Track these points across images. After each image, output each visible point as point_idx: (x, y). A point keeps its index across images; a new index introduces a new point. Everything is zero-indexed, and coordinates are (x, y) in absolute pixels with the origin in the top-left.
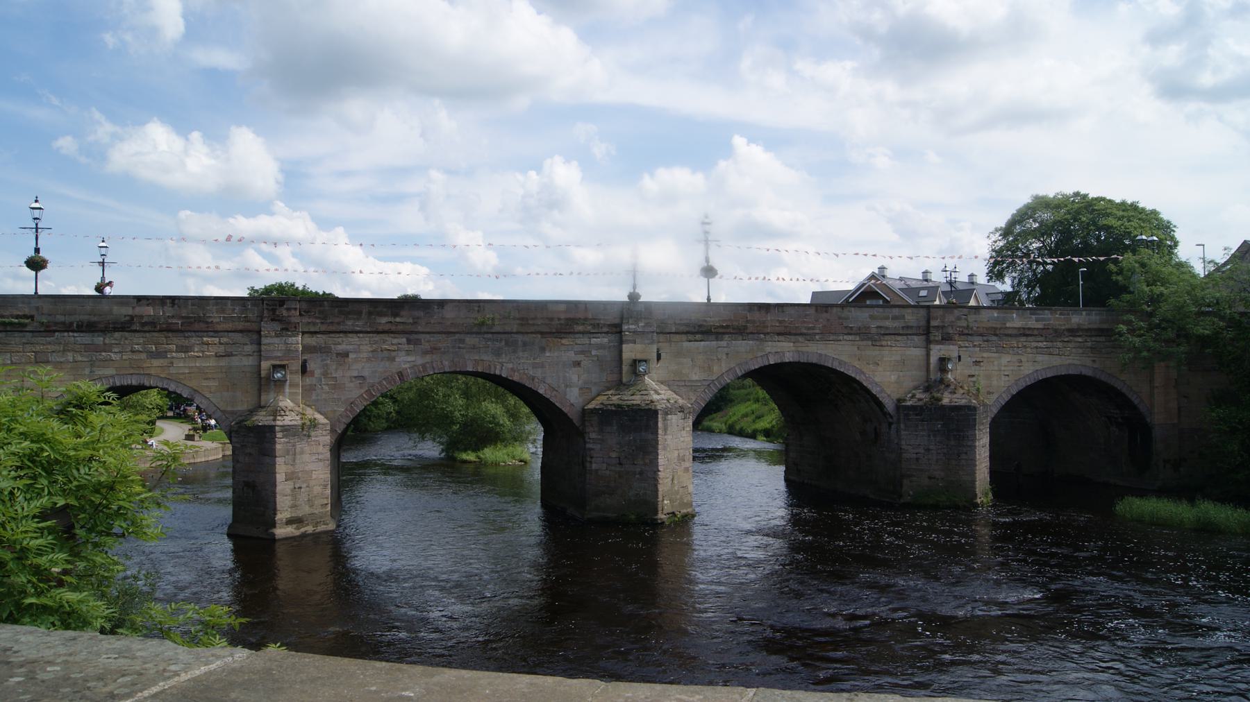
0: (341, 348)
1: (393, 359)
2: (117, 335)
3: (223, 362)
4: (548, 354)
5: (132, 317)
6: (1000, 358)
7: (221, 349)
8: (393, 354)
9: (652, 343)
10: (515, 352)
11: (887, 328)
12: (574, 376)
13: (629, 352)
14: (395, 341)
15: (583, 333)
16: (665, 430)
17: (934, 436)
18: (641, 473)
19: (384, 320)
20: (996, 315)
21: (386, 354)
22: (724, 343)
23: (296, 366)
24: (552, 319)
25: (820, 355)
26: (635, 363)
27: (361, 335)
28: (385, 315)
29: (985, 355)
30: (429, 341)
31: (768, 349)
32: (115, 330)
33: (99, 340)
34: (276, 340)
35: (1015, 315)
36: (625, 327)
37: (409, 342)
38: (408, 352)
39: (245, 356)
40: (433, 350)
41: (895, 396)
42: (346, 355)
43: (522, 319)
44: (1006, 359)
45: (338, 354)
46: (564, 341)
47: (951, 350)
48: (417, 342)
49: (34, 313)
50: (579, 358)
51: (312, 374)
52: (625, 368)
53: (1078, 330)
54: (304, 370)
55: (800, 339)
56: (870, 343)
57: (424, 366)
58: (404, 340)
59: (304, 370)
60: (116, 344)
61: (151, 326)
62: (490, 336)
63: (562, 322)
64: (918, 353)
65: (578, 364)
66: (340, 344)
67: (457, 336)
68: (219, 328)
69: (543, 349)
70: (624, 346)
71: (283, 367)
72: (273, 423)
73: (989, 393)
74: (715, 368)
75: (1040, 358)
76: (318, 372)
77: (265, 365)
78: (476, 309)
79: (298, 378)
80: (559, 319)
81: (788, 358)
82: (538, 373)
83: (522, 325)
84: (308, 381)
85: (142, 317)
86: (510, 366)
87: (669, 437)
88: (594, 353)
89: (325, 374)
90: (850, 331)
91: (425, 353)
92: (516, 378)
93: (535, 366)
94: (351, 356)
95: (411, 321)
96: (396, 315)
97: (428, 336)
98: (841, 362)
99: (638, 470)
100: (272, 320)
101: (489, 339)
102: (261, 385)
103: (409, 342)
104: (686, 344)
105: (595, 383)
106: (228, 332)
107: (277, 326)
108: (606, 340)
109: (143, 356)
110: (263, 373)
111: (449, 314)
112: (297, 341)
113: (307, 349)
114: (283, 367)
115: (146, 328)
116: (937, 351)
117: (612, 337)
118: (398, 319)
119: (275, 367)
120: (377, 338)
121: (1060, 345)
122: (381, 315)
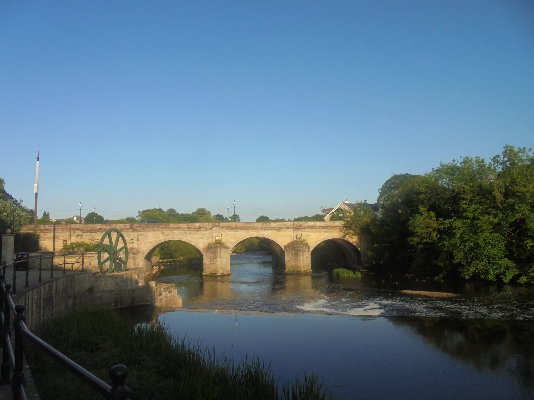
0: (146, 235)
1: (158, 237)
4: (194, 235)
5: (100, 229)
6: (314, 234)
8: (158, 236)
9: (220, 232)
10: (187, 235)
11: (282, 228)
12: (201, 240)
13: (214, 235)
16: (220, 253)
17: (292, 255)
18: (215, 263)
19: (156, 228)
20: (313, 223)
21: (156, 236)
23: (136, 239)
24: (196, 227)
25: (264, 235)
27: (151, 232)
28: (156, 227)
29: (310, 234)
30: (166, 233)
33: (94, 234)
35: (318, 223)
37: (162, 233)
38: (162, 236)
40: (168, 235)
41: (284, 245)
42: (148, 236)
43: (189, 227)
44: (316, 235)
45: (146, 236)
46: (199, 232)
49: (80, 228)
50: (202, 236)
51: (140, 241)
53: (337, 226)
54: (138, 240)
55: (258, 231)
56: (277, 231)
57: (165, 239)
58: (161, 233)
59: (138, 240)
62: (180, 231)
63: (198, 228)
65: (202, 238)
66: (146, 234)
67: (173, 232)
69: (193, 235)
71: (133, 239)
72: (130, 252)
73: (311, 244)
74: (236, 238)
75: (326, 234)
78: (178, 225)
80: (197, 227)
82: (192, 240)
83: (188, 229)
84: (139, 242)
85: (103, 228)
86: (186, 238)
87: (221, 255)
88: (206, 235)
89: (143, 241)
90: (271, 228)
91: (166, 235)
92: (187, 241)
93: (192, 238)
94: (148, 237)
95: (162, 228)
96: (159, 227)
98: (269, 236)
99: (214, 263)
100: (131, 229)
101: (180, 232)
103: (162, 233)
104: (229, 232)
105: (206, 242)
107: (132, 230)
108: (209, 232)
112: (136, 233)
114: (133, 239)
116: (295, 233)
117: (211, 231)
118: (159, 228)
119: (131, 239)
120: (155, 232)
121: (331, 230)
122: (155, 227)
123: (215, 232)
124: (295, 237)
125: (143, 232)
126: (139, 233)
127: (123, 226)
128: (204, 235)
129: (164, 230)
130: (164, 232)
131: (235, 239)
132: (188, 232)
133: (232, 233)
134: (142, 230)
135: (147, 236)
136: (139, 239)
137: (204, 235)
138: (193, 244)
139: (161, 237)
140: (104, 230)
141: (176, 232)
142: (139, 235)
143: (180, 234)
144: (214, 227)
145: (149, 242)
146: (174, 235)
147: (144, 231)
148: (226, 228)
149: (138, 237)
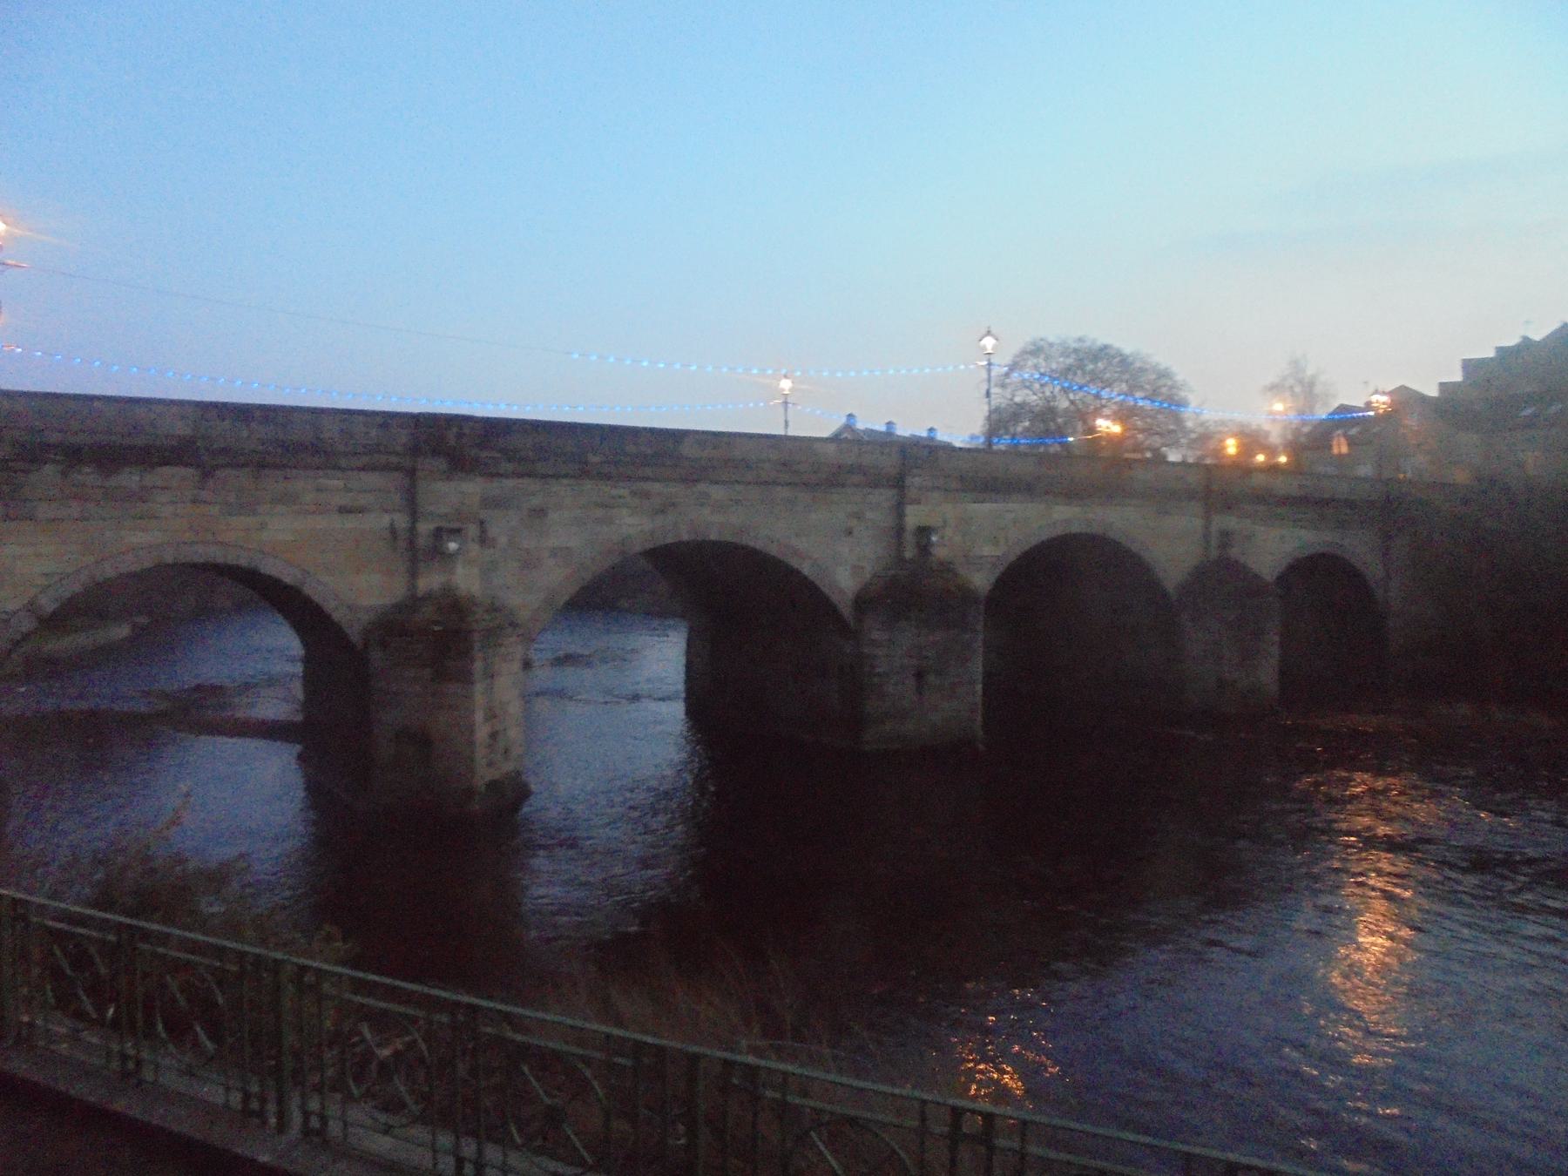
2: (167, 470)
3: (351, 522)
7: (345, 500)
13: (914, 516)
14: (615, 492)
15: (857, 486)
22: (1011, 506)
26: (924, 531)
27: (565, 481)
31: (1056, 516)
32: (165, 463)
34: (441, 487)
36: (908, 481)
37: (633, 493)
39: (386, 511)
47: (1231, 522)
48: (646, 495)
52: (909, 538)
59: (484, 540)
60: (163, 488)
61: (233, 458)
64: (1198, 523)
65: (850, 532)
67: (701, 487)
68: (343, 462)
70: (910, 510)
71: (458, 531)
76: (503, 540)
77: (425, 527)
79: (474, 548)
81: (1075, 528)
88: (869, 515)
97: (657, 487)
102: (414, 560)
106: (363, 469)
107: (441, 464)
109: (215, 510)
110: (422, 542)
111: (687, 449)
112: (472, 489)
113: (491, 503)
114: (458, 531)
115: (221, 460)
116: (1222, 521)
120: (588, 485)
123: (918, 502)
124: (1214, 542)
125: (510, 483)
126: (496, 487)
127: (373, 433)
128: (858, 516)
129: (648, 471)
130: (647, 486)
131: (995, 541)
132: (783, 492)
133: (983, 510)
134: (510, 467)
135: (540, 513)
136: (493, 531)
137: (858, 516)
138: (806, 569)
139: (630, 520)
140: (224, 451)
141: (718, 493)
142: (491, 503)
143: (737, 502)
144: (915, 471)
145: (554, 553)
146: (706, 511)
147: (520, 476)
148: (962, 478)
149: (483, 514)
